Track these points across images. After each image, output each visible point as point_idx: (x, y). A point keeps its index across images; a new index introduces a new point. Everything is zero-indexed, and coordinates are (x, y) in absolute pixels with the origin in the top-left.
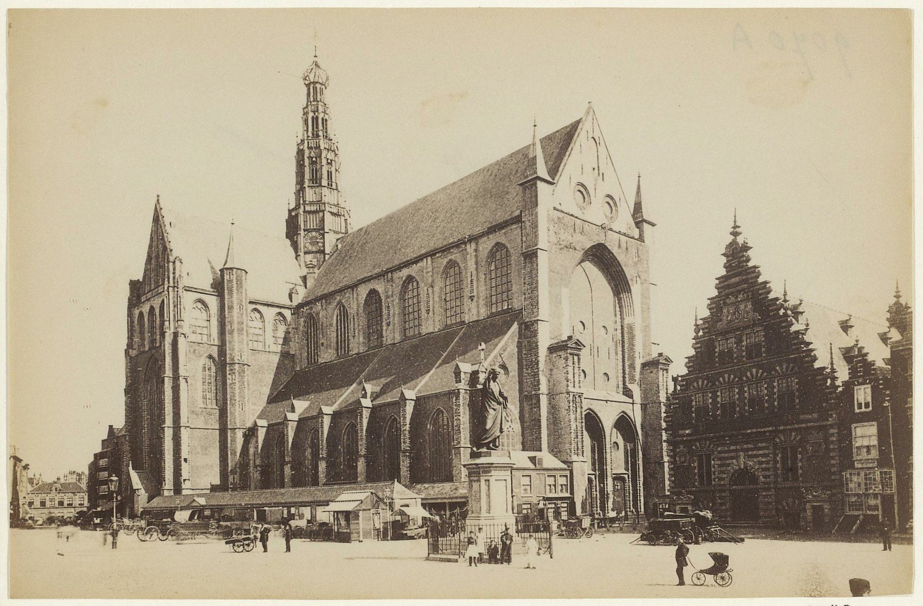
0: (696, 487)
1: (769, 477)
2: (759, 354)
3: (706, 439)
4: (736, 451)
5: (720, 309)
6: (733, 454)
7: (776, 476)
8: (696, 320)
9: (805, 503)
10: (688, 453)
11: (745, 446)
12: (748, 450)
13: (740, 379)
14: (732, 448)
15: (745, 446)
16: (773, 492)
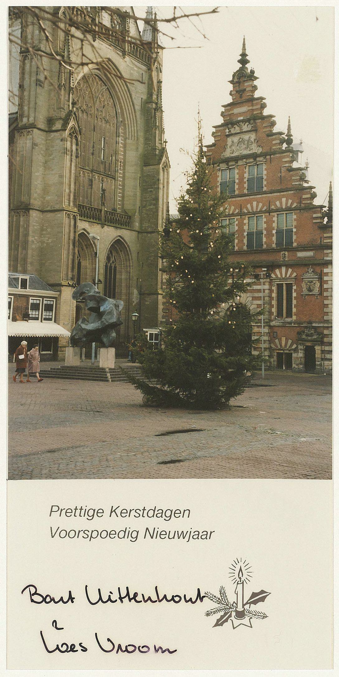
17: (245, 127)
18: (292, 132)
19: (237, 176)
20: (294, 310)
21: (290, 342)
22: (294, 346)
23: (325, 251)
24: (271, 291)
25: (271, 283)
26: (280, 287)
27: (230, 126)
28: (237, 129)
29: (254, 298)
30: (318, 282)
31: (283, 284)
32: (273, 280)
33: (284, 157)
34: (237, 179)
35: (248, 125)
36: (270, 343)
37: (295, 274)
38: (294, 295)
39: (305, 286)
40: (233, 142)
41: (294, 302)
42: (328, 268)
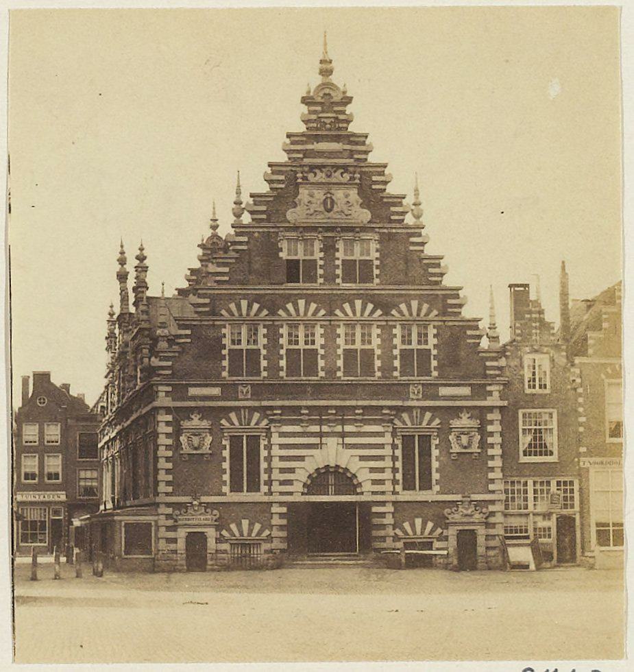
0: (225, 494)
1: (381, 482)
2: (367, 277)
3: (252, 410)
4: (321, 435)
5: (293, 184)
6: (315, 440)
7: (395, 482)
8: (238, 193)
9: (446, 526)
10: (211, 431)
11: (339, 428)
12: (343, 435)
13: (331, 313)
14: (315, 429)
15: (339, 428)
16: (389, 508)
17: (337, 177)
18: (421, 198)
19: (318, 255)
20: (436, 476)
21: (430, 525)
22: (439, 530)
23: (489, 388)
24: (394, 447)
25: (394, 434)
26: (408, 441)
27: (306, 169)
28: (320, 177)
29: (362, 458)
30: (477, 434)
31: (414, 436)
32: (398, 430)
33: (413, 235)
34: (321, 259)
35: (342, 174)
36: (394, 529)
37: (437, 421)
38: (435, 452)
39: (455, 440)
40: (312, 196)
41: (435, 465)
42: (492, 412)
